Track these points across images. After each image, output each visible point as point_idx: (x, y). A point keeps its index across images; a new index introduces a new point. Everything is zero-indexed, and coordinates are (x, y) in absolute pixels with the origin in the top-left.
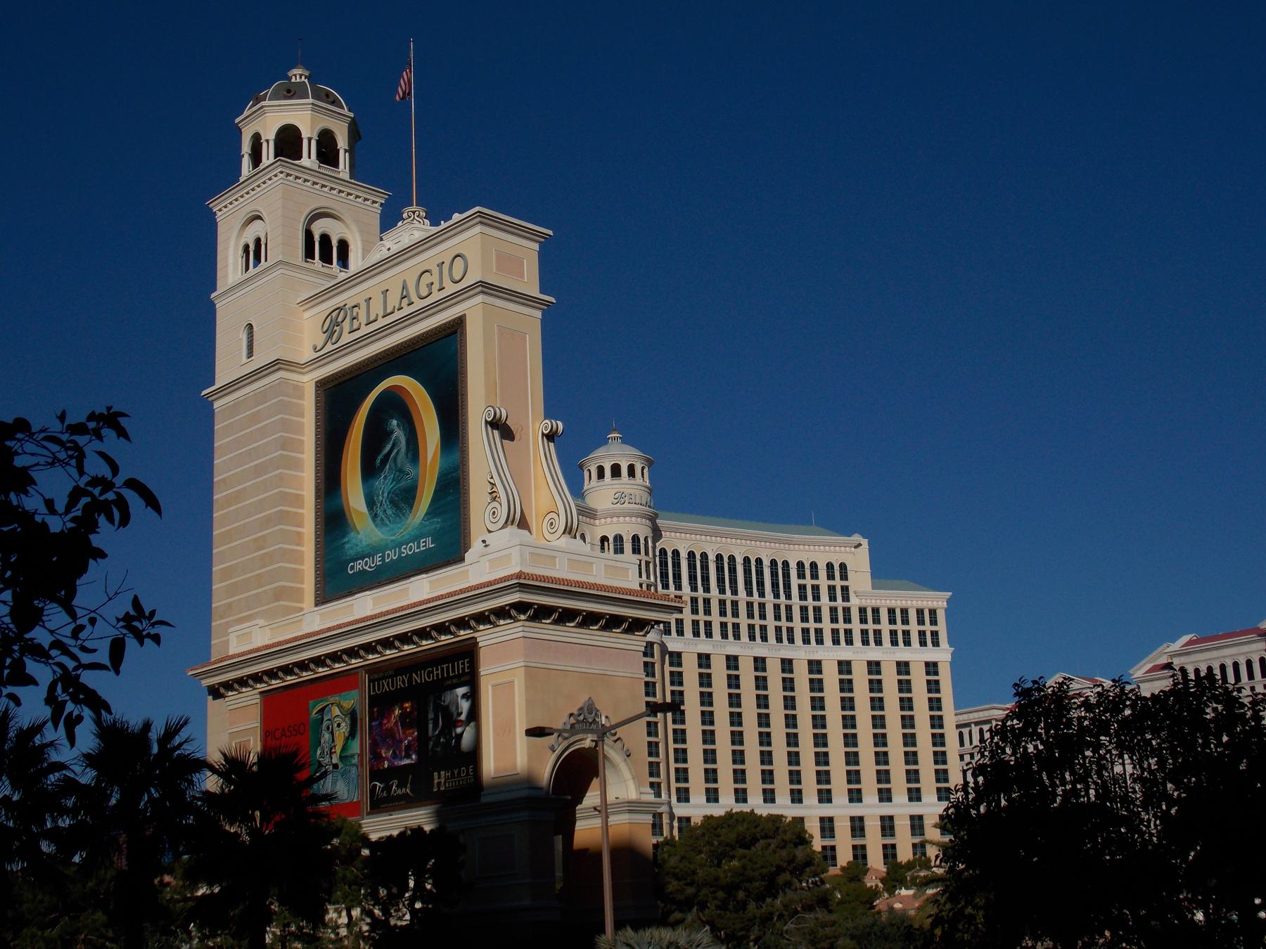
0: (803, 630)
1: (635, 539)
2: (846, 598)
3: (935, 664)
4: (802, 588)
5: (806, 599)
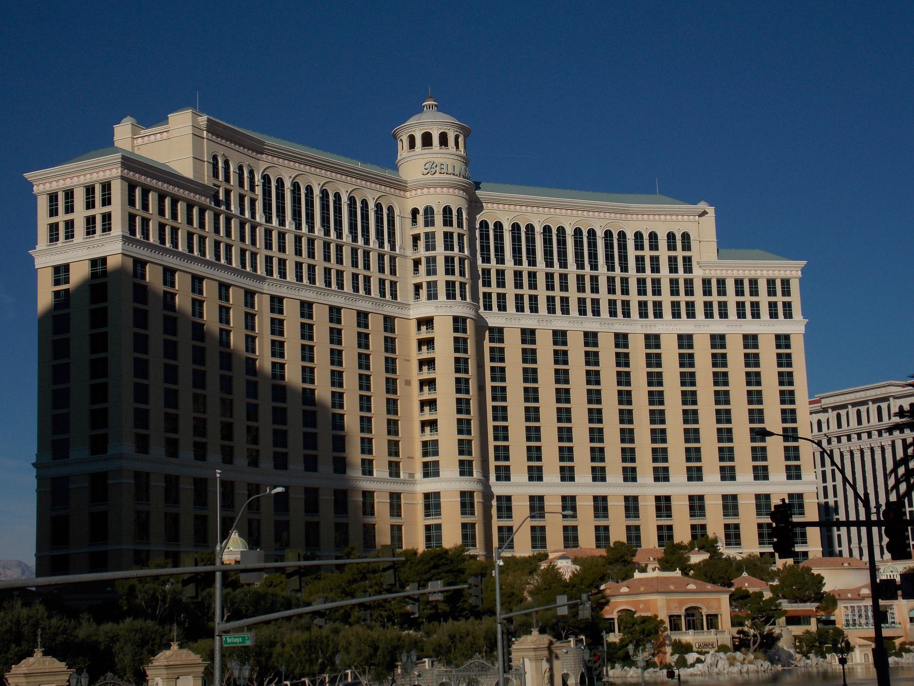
0: (640, 303)
1: (447, 211)
2: (688, 269)
3: (787, 337)
4: (640, 260)
5: (676, 271)
